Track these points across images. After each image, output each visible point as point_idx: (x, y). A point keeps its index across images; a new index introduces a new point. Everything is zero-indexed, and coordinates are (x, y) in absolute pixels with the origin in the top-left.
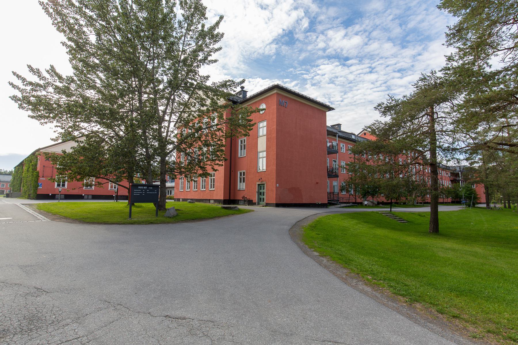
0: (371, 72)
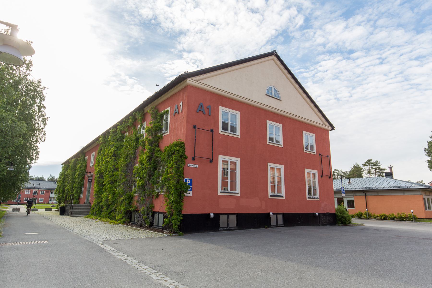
0: (381, 63)
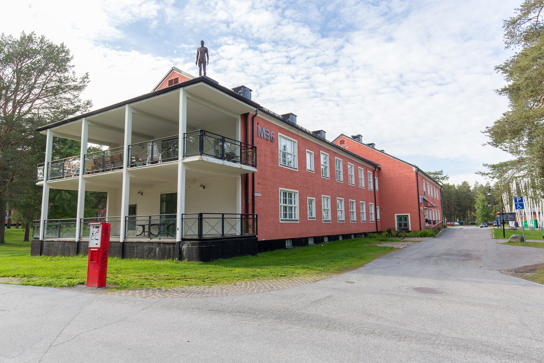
0: (289, 63)
